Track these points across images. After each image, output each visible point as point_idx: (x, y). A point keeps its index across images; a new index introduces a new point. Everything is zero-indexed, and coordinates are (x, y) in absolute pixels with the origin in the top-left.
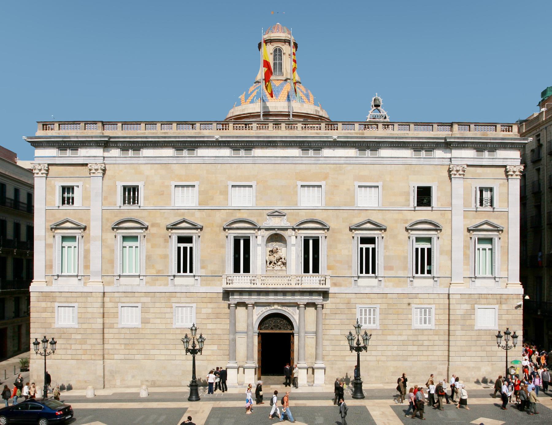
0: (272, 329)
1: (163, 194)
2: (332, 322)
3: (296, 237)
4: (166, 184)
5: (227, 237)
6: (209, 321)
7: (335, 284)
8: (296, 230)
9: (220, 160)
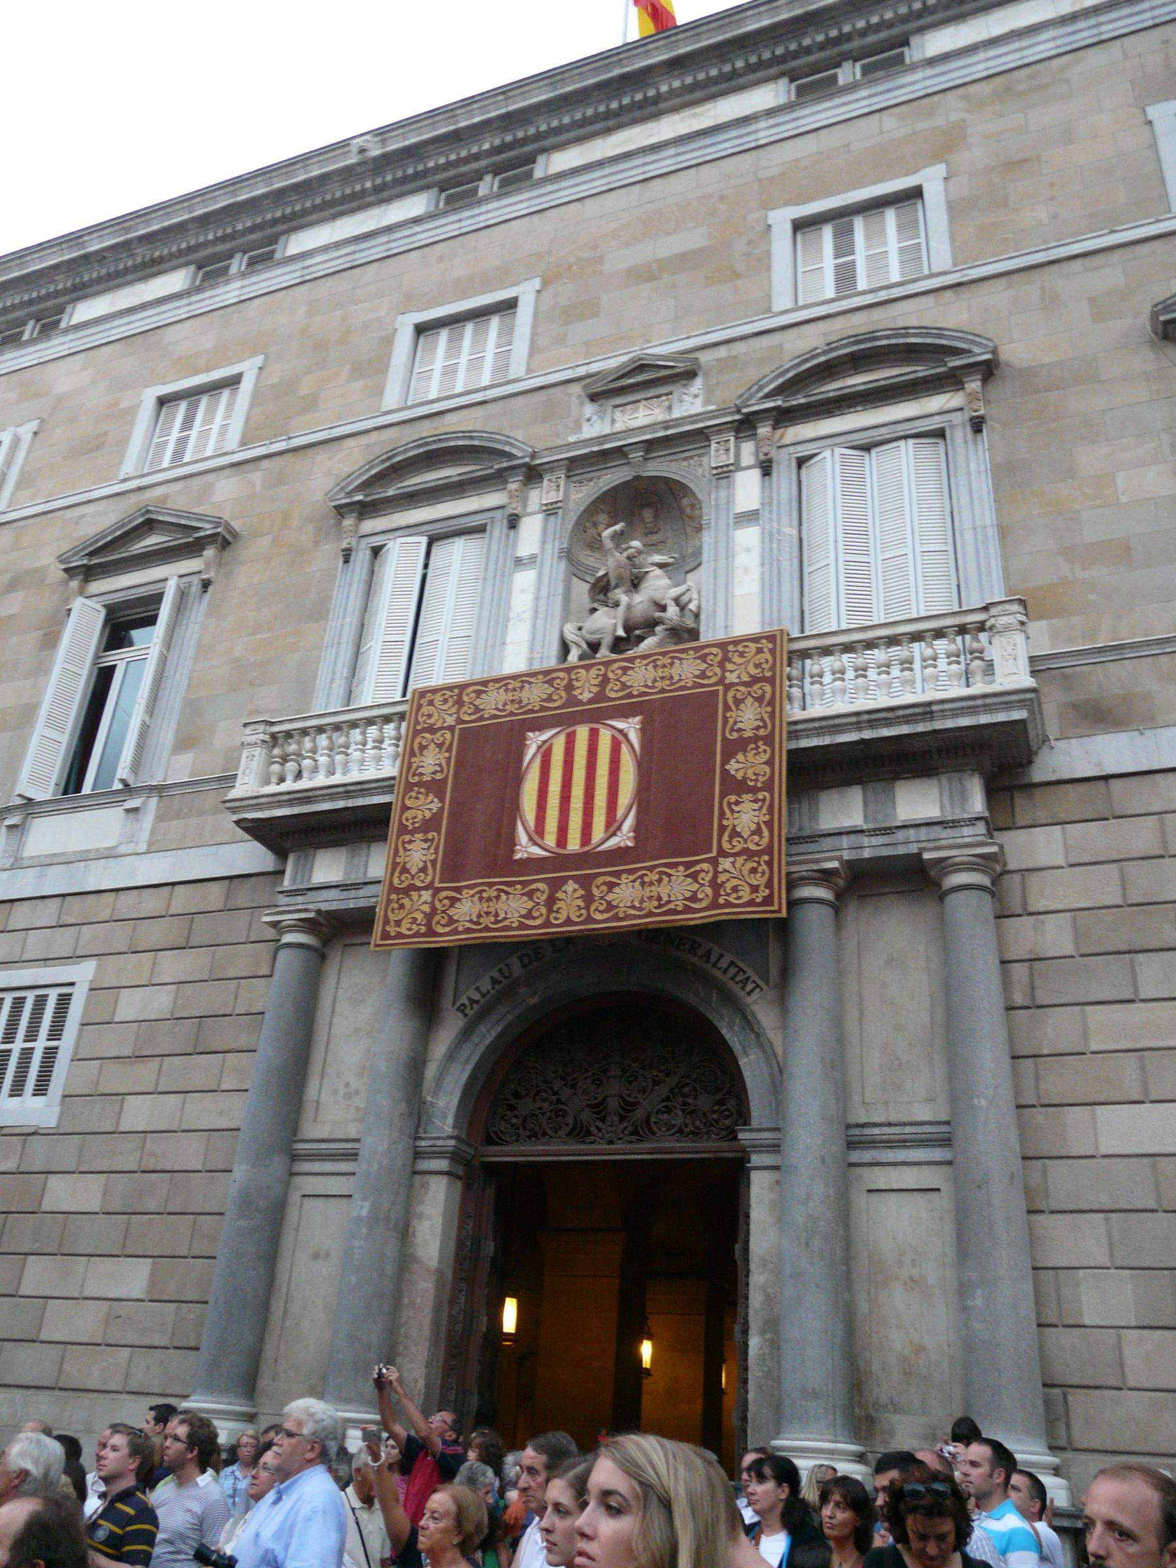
0: (580, 1133)
1: (99, 447)
2: (1109, 1027)
3: (766, 468)
4: (123, 405)
5: (347, 555)
6: (145, 1074)
7: (1099, 716)
8: (764, 430)
9: (376, 249)
